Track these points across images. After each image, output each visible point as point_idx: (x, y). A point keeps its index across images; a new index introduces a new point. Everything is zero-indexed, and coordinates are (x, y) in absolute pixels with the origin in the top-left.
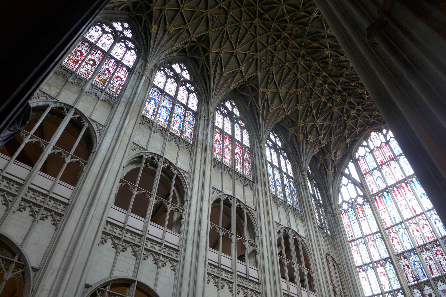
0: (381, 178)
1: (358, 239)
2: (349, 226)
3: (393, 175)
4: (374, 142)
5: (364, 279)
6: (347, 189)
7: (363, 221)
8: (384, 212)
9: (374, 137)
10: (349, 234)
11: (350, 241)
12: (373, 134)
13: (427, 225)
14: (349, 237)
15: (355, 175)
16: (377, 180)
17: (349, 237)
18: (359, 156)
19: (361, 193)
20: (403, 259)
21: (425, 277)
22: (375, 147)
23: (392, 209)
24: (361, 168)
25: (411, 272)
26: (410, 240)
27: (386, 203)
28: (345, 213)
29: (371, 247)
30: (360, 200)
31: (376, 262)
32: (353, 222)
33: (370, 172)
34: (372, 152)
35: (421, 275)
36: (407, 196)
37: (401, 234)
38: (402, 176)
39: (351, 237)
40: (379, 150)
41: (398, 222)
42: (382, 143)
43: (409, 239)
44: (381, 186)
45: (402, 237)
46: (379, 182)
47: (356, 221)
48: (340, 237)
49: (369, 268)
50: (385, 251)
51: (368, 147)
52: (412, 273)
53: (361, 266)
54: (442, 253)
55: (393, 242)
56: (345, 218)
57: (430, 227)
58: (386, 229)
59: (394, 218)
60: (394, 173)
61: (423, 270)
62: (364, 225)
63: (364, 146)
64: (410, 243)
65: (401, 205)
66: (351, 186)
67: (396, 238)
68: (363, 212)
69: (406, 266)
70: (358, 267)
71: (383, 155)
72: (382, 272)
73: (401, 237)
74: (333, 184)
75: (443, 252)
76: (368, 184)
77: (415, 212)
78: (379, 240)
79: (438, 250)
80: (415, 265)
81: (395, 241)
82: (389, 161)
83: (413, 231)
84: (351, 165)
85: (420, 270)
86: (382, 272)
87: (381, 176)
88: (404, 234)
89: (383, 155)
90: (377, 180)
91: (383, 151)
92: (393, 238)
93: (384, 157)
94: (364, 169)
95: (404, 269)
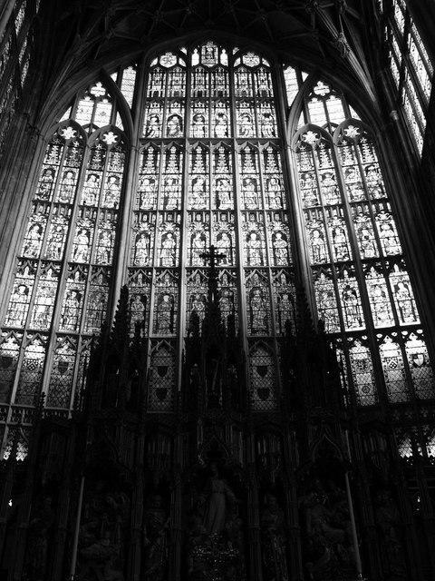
0: (181, 121)
1: (57, 205)
2: (53, 175)
3: (209, 125)
4: (203, 58)
5: (22, 289)
6: (95, 107)
7: (93, 177)
8: (152, 181)
9: (210, 50)
10: (42, 189)
11: (36, 203)
12: (210, 47)
13: (229, 236)
14: (40, 194)
15: (127, 93)
16: (169, 120)
17: (40, 194)
18: (159, 65)
19: (119, 124)
20: (140, 281)
21: (172, 332)
22: (200, 64)
23: (170, 182)
24: (149, 87)
25: (145, 312)
26: (177, 250)
27: (164, 165)
28: (60, 146)
29: (80, 233)
30: (110, 139)
31: (74, 265)
32: (67, 169)
33: (161, 101)
34: (188, 70)
35: (164, 324)
36: (217, 171)
37: (164, 233)
38: (227, 134)
39: (45, 195)
40: (205, 73)
41: (169, 207)
42: (220, 65)
43: (175, 249)
44: (172, 132)
45: (163, 240)
46: (173, 125)
47: (76, 171)
48: (18, 178)
49: (50, 271)
50: (109, 253)
51: (188, 59)
52: (144, 315)
53: (35, 261)
54: (232, 297)
55: (137, 241)
56: (53, 154)
57: (234, 242)
58: (137, 213)
59: (166, 199)
60: (213, 122)
61: (175, 316)
62: (90, 184)
63: (180, 55)
64: (174, 255)
65: (195, 181)
66: (106, 107)
67: (148, 237)
68: (103, 162)
69: (139, 297)
70: (23, 260)
71: (210, 85)
72: (77, 291)
73: (160, 239)
74: (68, 77)
75: (235, 296)
76: (146, 118)
77: (218, 203)
78: (107, 226)
79: (228, 288)
80: (161, 300)
81: (143, 242)
82: (215, 100)
83: (193, 236)
84: (129, 75)
85: (169, 314)
86: (77, 291)
87: (183, 116)
88: (169, 236)
89: (210, 85)
90: (169, 120)
91: (213, 78)
92: (141, 234)
93: (210, 89)
94: (154, 89)
95: (132, 300)
